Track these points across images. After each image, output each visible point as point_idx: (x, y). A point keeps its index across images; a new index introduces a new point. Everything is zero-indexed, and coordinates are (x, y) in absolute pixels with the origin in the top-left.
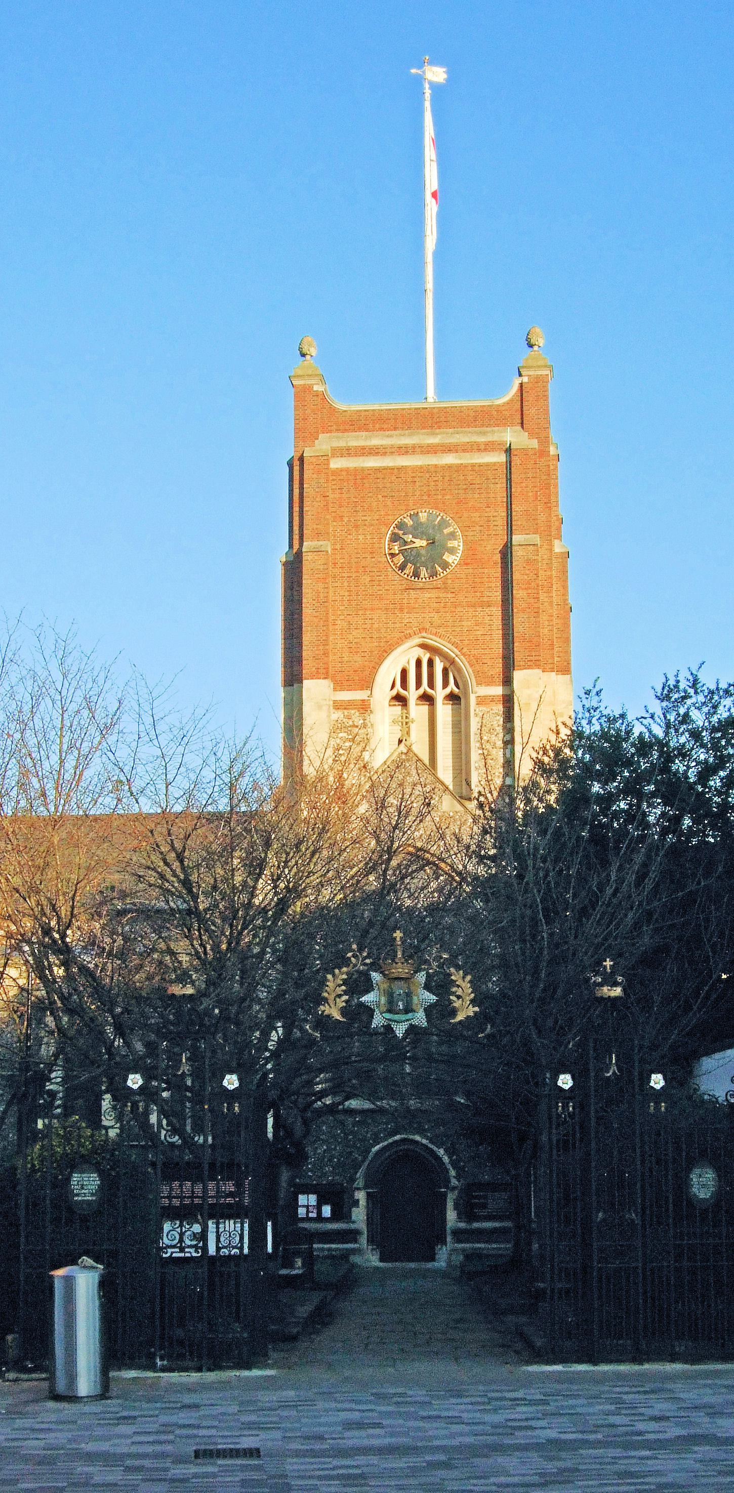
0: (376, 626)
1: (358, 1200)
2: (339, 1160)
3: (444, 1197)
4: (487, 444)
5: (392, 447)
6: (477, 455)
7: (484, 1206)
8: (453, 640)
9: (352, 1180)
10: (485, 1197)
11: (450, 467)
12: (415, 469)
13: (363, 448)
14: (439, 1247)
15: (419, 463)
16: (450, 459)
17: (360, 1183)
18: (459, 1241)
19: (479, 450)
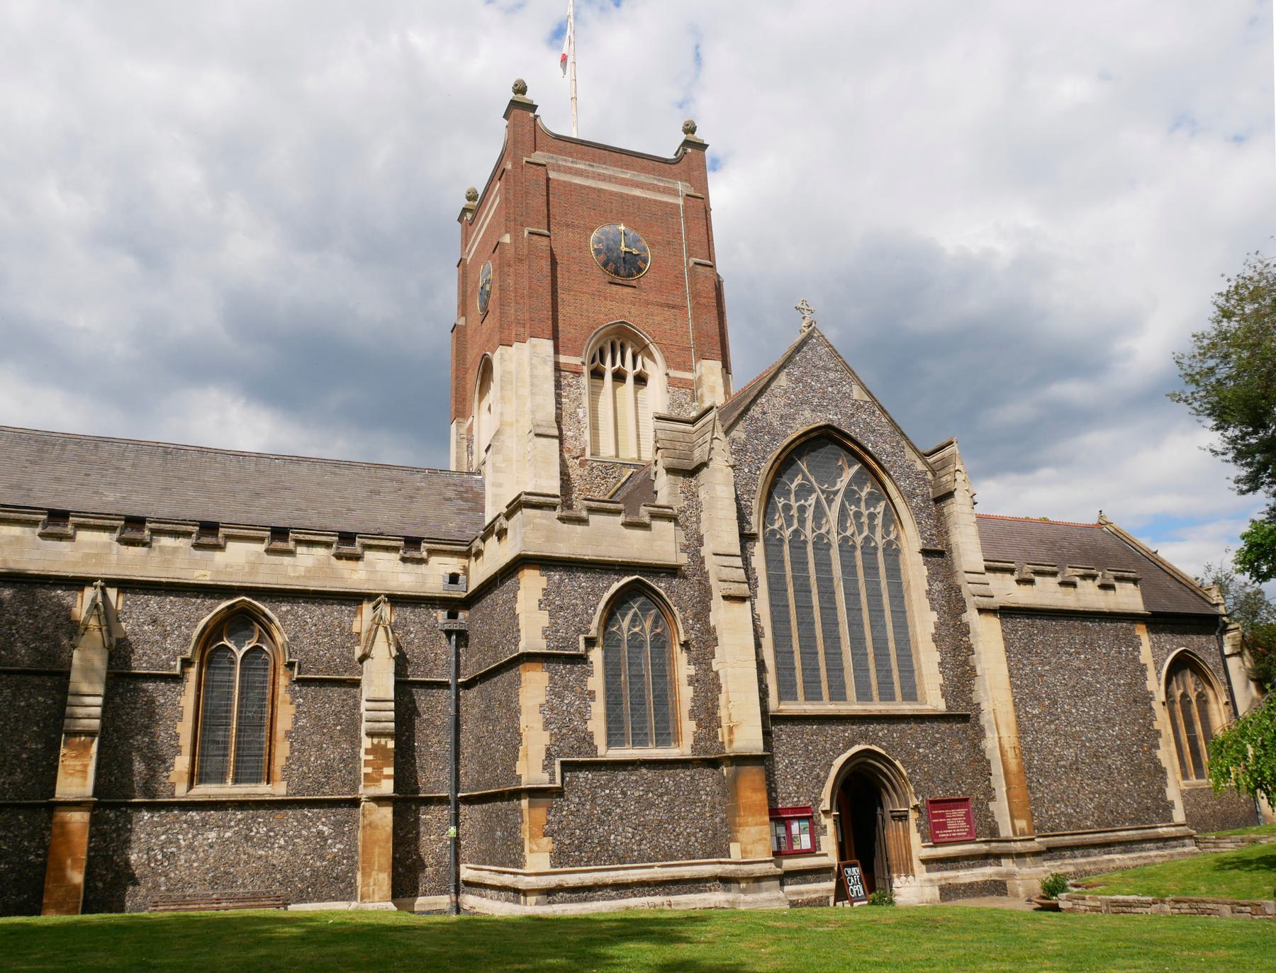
0: (585, 306)
1: (826, 827)
2: (801, 777)
3: (903, 817)
4: (665, 188)
5: (594, 173)
6: (658, 194)
7: (944, 826)
8: (647, 329)
9: (818, 801)
10: (943, 816)
11: (639, 198)
12: (611, 193)
13: (571, 168)
14: (903, 878)
15: (615, 190)
16: (637, 192)
17: (826, 805)
18: (928, 871)
19: (659, 191)
